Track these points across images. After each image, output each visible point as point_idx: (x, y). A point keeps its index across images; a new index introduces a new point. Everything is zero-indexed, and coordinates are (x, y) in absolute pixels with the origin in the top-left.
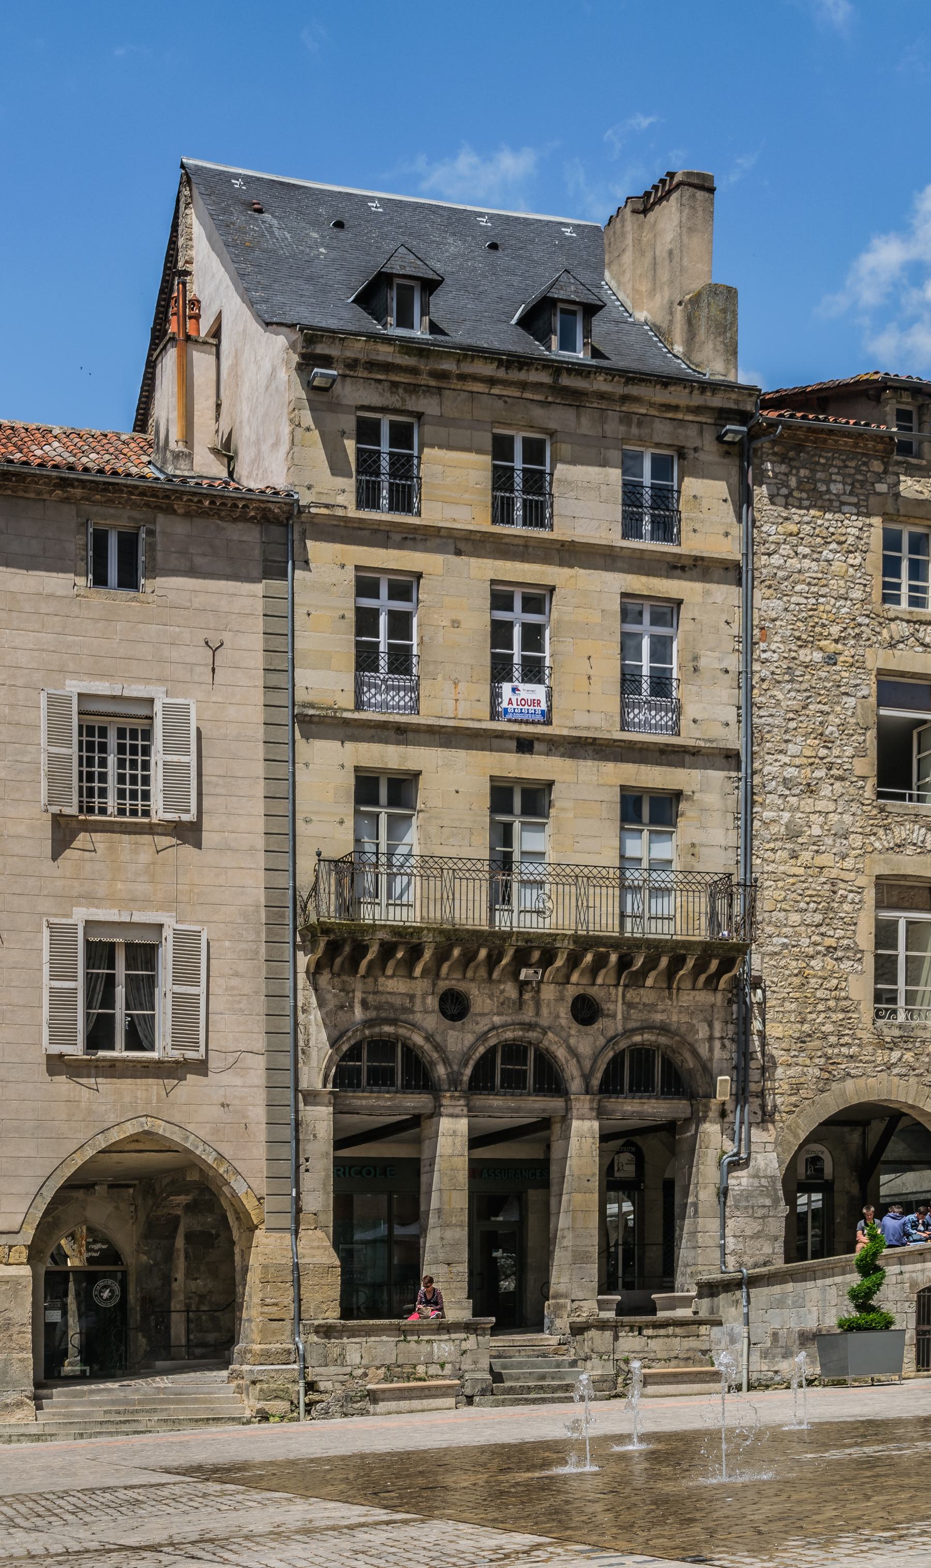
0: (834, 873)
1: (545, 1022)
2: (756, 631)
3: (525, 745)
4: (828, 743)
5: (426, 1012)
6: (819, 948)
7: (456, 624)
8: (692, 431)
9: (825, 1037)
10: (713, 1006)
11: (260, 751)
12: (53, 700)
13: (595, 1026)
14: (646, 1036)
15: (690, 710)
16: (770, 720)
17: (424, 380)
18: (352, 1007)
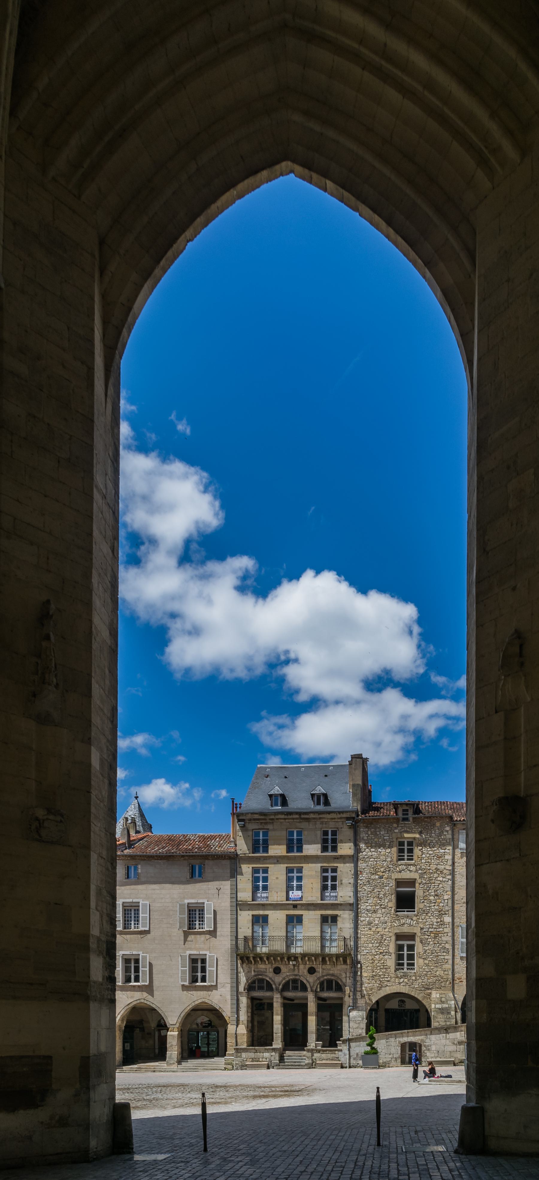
0: (382, 933)
1: (300, 974)
2: (359, 872)
3: (295, 906)
4: (380, 899)
5: (270, 972)
6: (378, 953)
7: (277, 878)
8: (340, 823)
9: (380, 976)
10: (346, 969)
11: (229, 913)
12: (180, 905)
13: (314, 975)
14: (328, 977)
15: (340, 894)
16: (363, 895)
17: (268, 821)
18: (251, 972)
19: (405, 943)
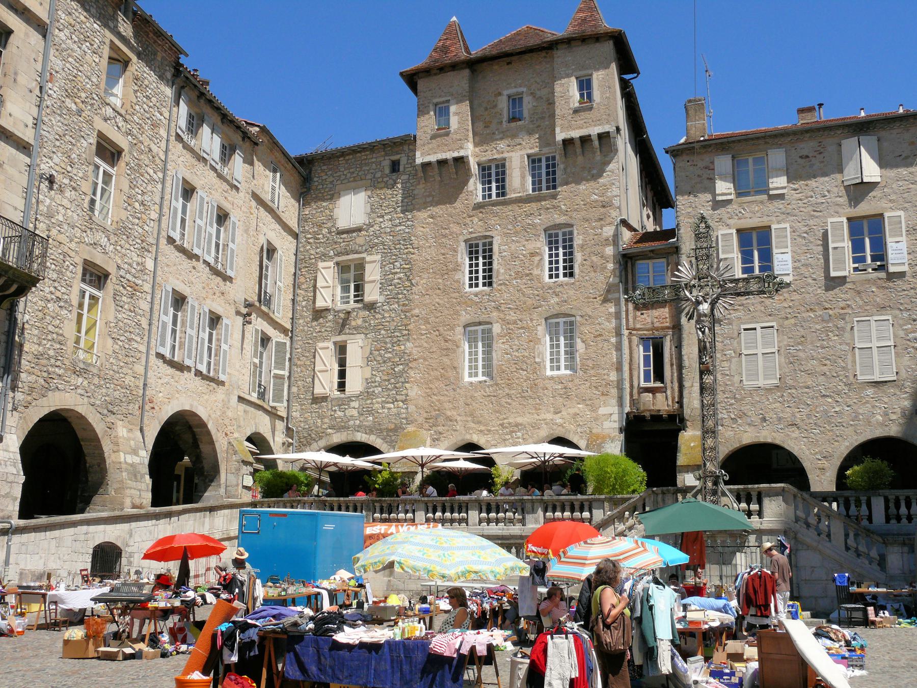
0: (66, 249)
6: (53, 297)
19: (90, 290)
